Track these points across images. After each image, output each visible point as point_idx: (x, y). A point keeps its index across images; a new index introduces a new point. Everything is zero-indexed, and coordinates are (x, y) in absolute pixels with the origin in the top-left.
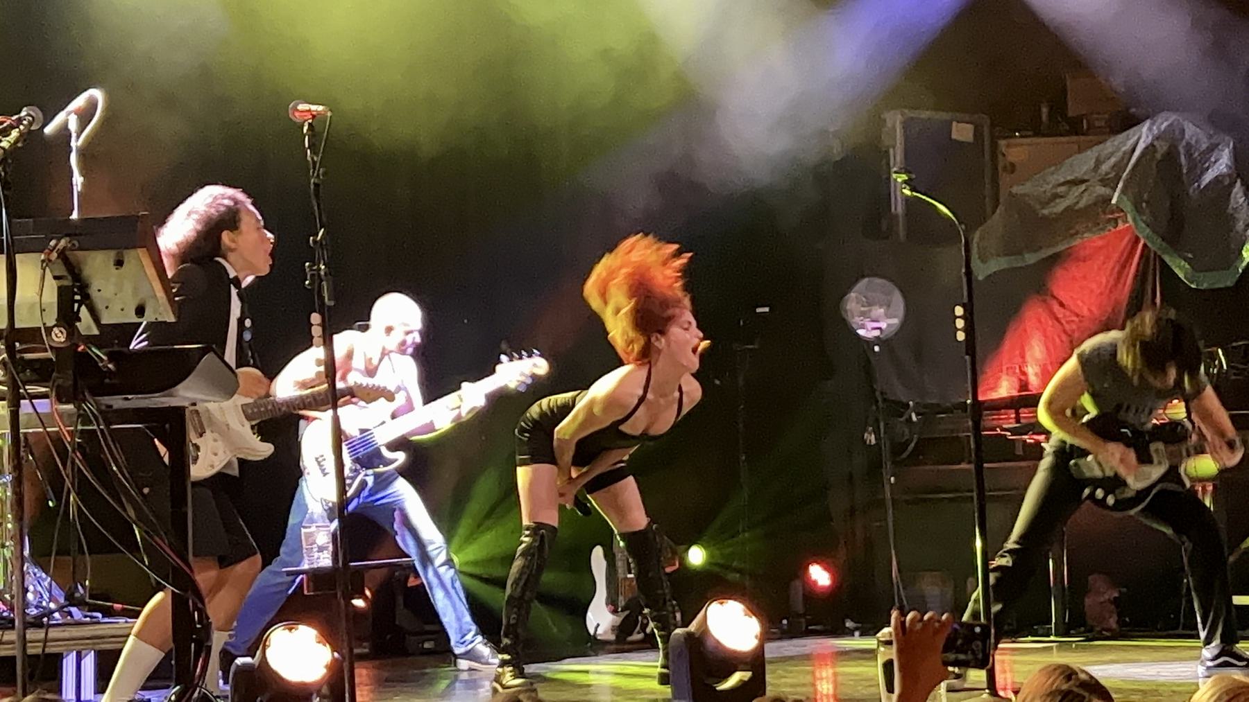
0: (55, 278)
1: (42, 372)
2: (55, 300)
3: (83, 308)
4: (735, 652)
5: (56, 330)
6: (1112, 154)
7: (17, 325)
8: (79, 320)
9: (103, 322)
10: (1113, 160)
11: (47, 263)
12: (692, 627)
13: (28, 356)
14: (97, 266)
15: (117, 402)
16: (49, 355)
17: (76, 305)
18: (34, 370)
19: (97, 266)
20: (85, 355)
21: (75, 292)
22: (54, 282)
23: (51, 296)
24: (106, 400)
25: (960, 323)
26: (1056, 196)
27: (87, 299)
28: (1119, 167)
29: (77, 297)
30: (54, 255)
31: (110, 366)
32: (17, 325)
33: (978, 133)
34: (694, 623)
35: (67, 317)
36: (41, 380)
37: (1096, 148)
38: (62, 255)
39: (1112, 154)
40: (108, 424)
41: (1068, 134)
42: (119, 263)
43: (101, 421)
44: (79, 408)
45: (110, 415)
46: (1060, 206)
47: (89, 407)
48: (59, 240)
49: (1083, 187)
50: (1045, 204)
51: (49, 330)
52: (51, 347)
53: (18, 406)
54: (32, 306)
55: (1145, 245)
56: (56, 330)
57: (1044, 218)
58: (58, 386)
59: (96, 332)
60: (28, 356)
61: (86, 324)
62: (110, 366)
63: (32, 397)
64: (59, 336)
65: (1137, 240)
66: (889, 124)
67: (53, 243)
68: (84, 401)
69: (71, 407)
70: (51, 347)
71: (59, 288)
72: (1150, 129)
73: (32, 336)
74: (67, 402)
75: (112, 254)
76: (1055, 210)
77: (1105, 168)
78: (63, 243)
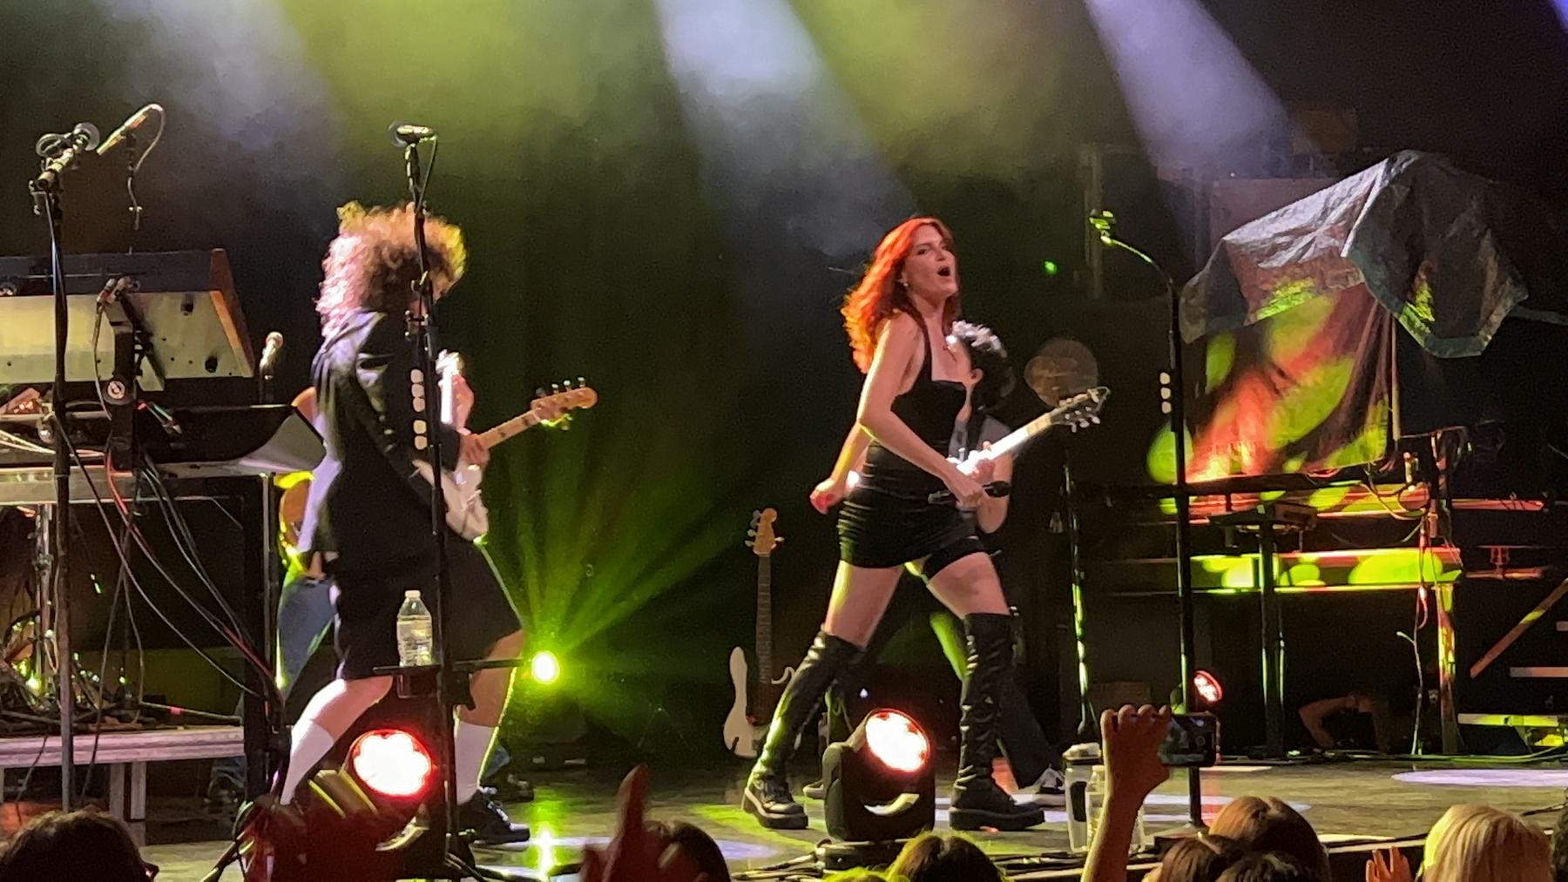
0: (113, 324)
1: (95, 434)
2: (113, 349)
3: (145, 359)
5: (113, 385)
7: (68, 379)
8: (140, 373)
9: (169, 376)
10: (1344, 206)
12: (851, 742)
13: (79, 415)
14: (163, 311)
15: (183, 470)
16: (105, 413)
17: (137, 356)
18: (86, 432)
19: (163, 311)
21: (134, 343)
22: (112, 330)
23: (107, 345)
24: (171, 467)
25: (1166, 393)
26: (1275, 249)
27: (149, 350)
28: (1350, 214)
29: (139, 347)
30: (113, 296)
31: (176, 428)
32: (68, 379)
34: (853, 736)
35: (126, 370)
36: (95, 441)
37: (1325, 192)
38: (122, 298)
40: (172, 495)
42: (188, 308)
43: (164, 491)
44: (138, 477)
45: (173, 486)
47: (151, 475)
48: (117, 279)
49: (1308, 238)
51: (104, 385)
53: (68, 473)
54: (84, 355)
55: (1379, 306)
56: (113, 385)
59: (159, 387)
60: (79, 415)
61: (148, 379)
62: (176, 428)
63: (84, 462)
64: (116, 392)
65: (1370, 299)
67: (110, 283)
68: (145, 467)
69: (129, 474)
72: (1388, 170)
73: (86, 391)
75: (179, 299)
76: (1275, 264)
77: (1334, 216)
78: (121, 282)
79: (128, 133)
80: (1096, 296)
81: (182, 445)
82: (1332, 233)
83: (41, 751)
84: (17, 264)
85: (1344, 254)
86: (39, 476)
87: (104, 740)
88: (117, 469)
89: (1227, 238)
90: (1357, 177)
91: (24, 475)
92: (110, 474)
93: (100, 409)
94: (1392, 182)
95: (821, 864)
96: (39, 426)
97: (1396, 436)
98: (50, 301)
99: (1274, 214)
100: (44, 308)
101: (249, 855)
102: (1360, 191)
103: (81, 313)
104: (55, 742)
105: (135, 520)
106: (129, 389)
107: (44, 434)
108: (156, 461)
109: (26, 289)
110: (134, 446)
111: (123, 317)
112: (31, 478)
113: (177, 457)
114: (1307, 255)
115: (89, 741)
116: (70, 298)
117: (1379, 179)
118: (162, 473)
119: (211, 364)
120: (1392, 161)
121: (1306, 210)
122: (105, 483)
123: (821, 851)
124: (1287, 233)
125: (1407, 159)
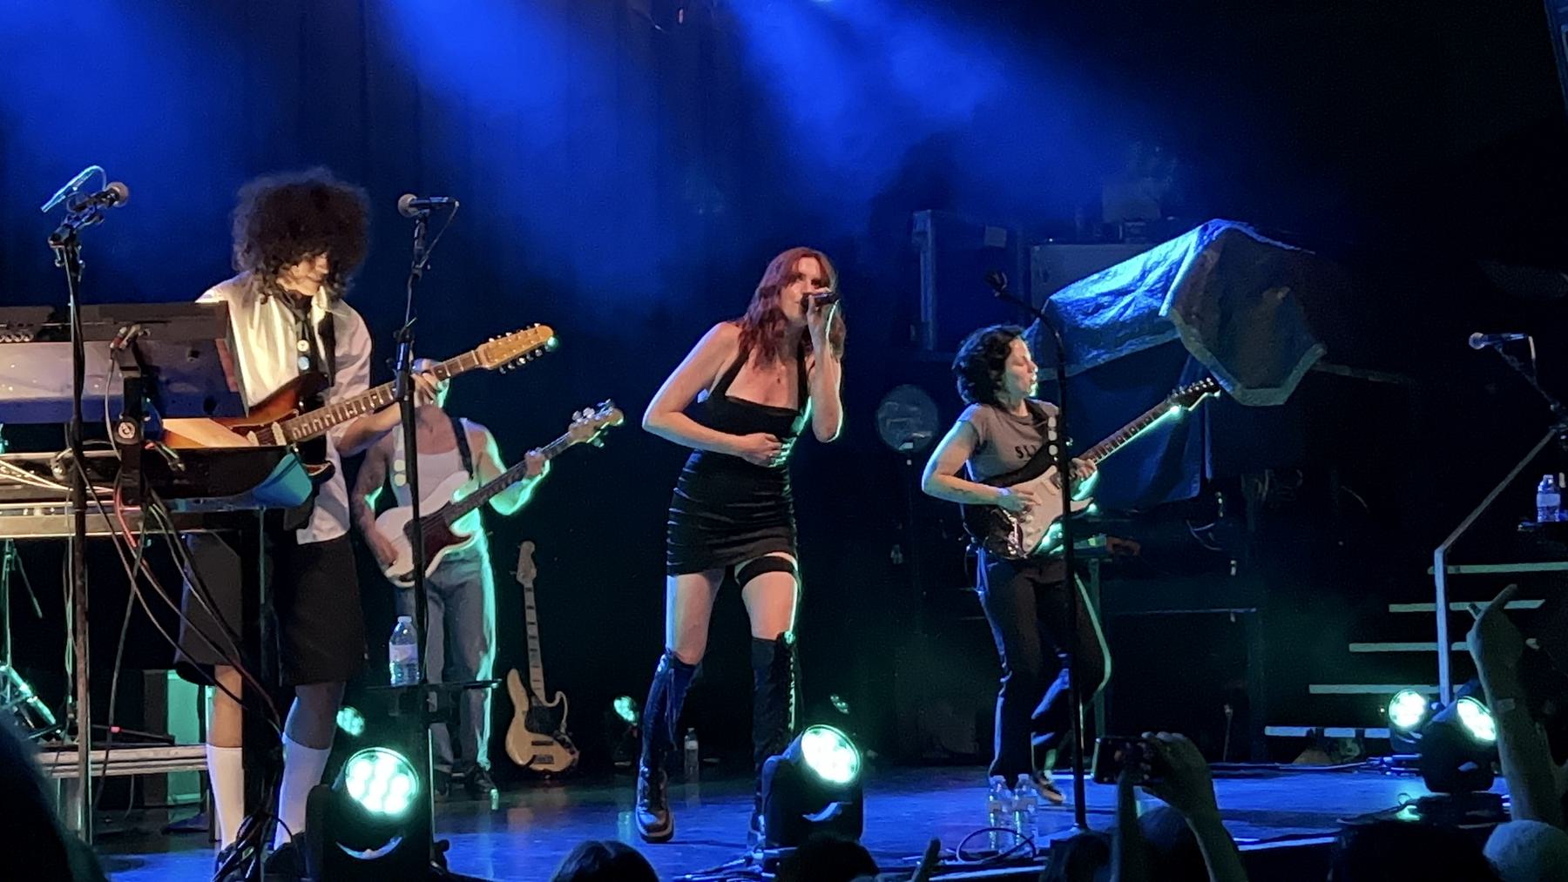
0: (123, 369)
1: (106, 471)
2: (120, 392)
4: (832, 783)
6: (1158, 264)
7: (85, 419)
11: (116, 354)
12: (787, 755)
13: (87, 453)
15: (182, 506)
16: (114, 453)
18: (94, 469)
20: (152, 451)
23: (118, 391)
26: (1099, 308)
28: (1168, 277)
30: (125, 342)
33: (1011, 237)
34: (789, 750)
36: (106, 479)
37: (1142, 257)
39: (1158, 264)
40: (177, 528)
41: (1102, 241)
44: (145, 510)
46: (1112, 313)
47: (157, 510)
48: (129, 327)
49: (1127, 299)
50: (1087, 315)
52: (117, 444)
57: (1089, 330)
58: (124, 489)
60: (87, 453)
63: (100, 497)
66: (918, 228)
67: (123, 331)
70: (117, 444)
71: (126, 381)
74: (133, 505)
76: (1098, 321)
77: (1152, 278)
78: (134, 329)
79: (70, 190)
80: (930, 348)
81: (185, 482)
82: (1151, 292)
83: (105, 762)
84: (40, 314)
85: (1163, 312)
86: (46, 511)
87: (113, 755)
88: (126, 504)
89: (1054, 297)
90: (1173, 242)
91: (31, 510)
92: (119, 509)
93: (110, 448)
94: (1206, 247)
95: (757, 868)
96: (53, 464)
97: (1209, 475)
98: (70, 345)
99: (1096, 276)
100: (62, 354)
101: (248, 861)
102: (1175, 256)
103: (97, 358)
104: (74, 757)
105: (147, 553)
106: (137, 432)
107: (57, 471)
108: (162, 496)
109: (38, 338)
110: (142, 482)
111: (134, 364)
112: (38, 513)
113: (184, 493)
114: (1129, 312)
115: (101, 755)
116: (87, 345)
117: (1193, 245)
118: (169, 510)
119: (767, 399)
120: (1205, 229)
121: (1125, 272)
122: (118, 520)
123: (759, 856)
124: (1110, 293)
125: (1219, 227)
